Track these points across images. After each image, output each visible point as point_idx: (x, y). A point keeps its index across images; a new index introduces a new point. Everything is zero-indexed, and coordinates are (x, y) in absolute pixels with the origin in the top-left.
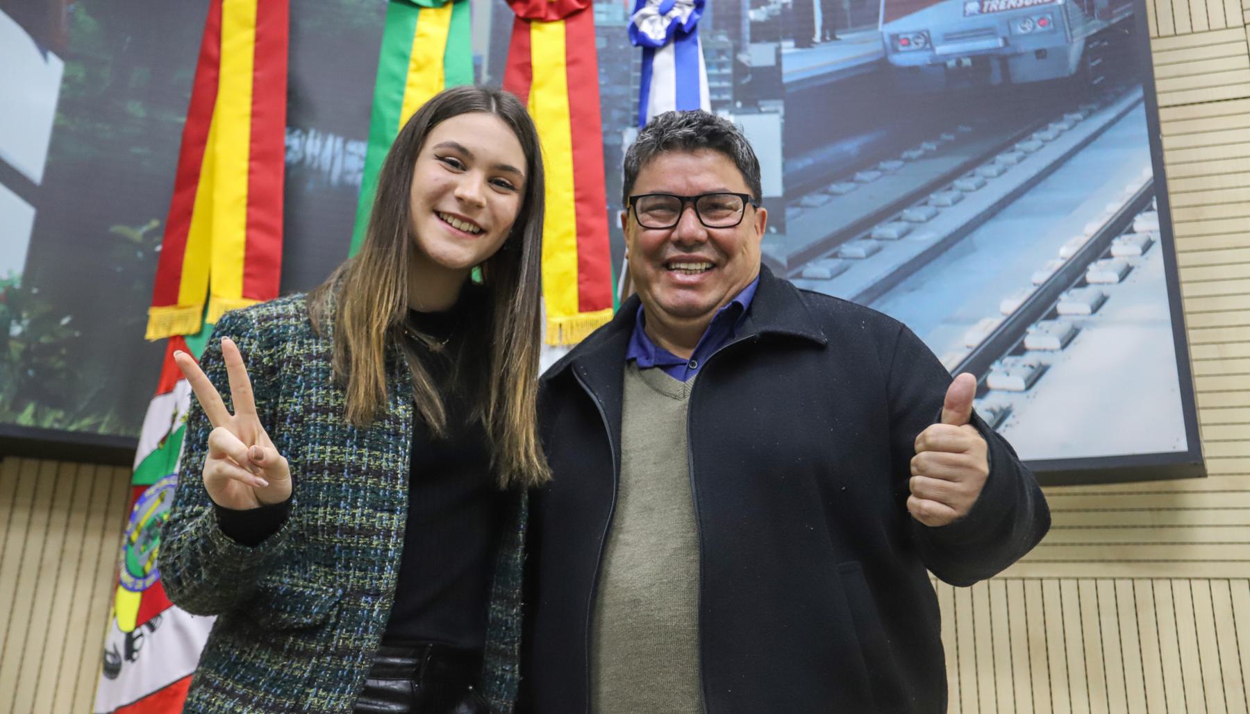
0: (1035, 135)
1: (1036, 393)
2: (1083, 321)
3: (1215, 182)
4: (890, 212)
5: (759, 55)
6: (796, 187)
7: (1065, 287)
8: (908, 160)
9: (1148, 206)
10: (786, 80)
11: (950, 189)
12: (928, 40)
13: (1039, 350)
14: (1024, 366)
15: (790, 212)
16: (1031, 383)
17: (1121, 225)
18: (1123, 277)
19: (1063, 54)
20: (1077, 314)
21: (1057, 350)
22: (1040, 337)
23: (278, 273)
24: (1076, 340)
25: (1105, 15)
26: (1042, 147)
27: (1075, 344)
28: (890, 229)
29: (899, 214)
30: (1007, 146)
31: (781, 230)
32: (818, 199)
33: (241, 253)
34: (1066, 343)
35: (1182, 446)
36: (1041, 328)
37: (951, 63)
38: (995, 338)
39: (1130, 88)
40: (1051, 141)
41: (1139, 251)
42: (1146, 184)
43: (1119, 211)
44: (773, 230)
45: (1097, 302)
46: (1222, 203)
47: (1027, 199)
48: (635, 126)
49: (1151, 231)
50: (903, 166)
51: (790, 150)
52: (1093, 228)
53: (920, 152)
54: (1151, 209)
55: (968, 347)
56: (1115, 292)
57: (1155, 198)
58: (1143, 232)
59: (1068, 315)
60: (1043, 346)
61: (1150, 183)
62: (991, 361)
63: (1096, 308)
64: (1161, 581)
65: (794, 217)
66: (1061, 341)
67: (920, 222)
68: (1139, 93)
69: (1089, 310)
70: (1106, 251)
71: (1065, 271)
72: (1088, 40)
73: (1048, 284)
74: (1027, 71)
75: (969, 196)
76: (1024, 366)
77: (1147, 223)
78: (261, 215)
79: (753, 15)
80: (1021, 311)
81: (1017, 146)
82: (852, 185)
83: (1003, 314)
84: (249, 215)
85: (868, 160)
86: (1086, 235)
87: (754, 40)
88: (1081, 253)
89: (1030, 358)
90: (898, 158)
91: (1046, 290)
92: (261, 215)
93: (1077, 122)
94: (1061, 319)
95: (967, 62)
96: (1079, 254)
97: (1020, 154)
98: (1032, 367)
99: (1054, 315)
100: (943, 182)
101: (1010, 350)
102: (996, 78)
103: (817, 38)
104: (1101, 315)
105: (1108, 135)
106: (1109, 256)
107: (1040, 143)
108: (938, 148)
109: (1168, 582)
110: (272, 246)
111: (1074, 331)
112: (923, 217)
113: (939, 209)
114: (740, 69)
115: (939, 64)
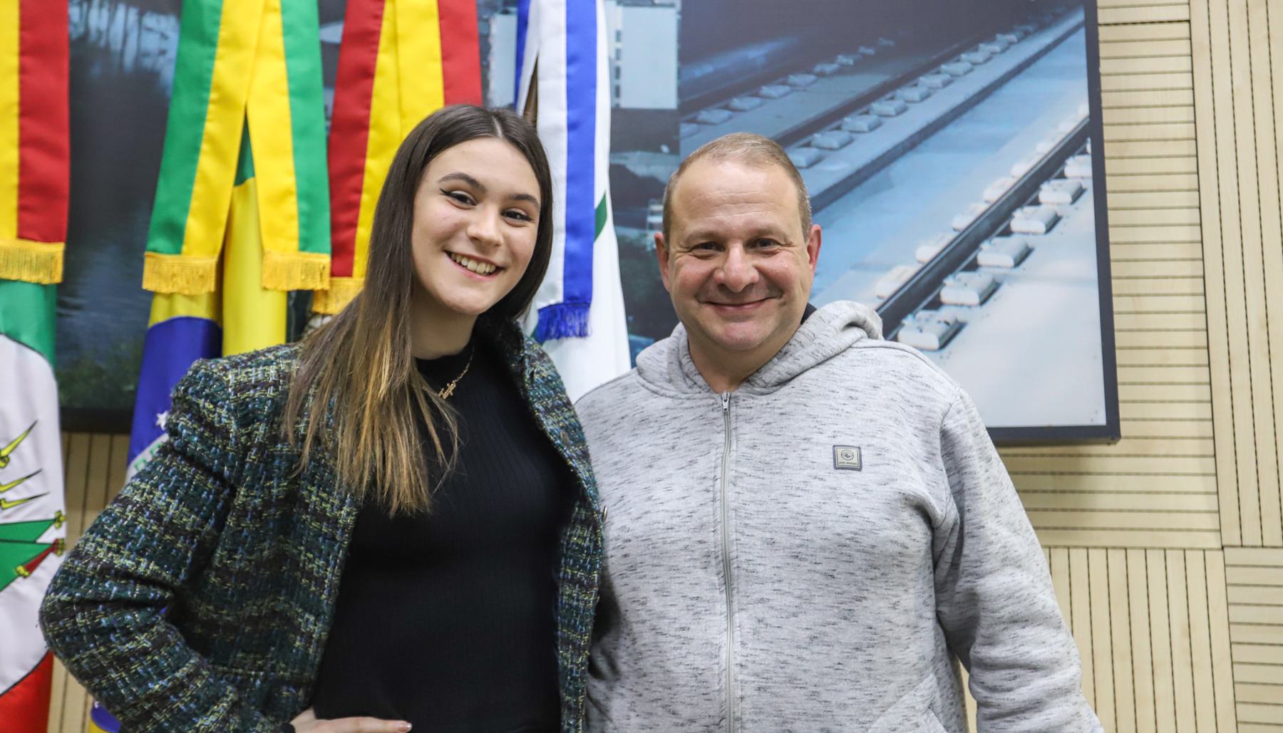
0: (963, 56)
1: (950, 353)
2: (1005, 275)
3: (1143, 115)
7: (987, 235)
8: (821, 75)
9: (1081, 149)
11: (867, 113)
13: (956, 305)
14: (939, 322)
15: (685, 129)
16: (945, 342)
18: (1050, 228)
20: (998, 267)
21: (976, 306)
22: (960, 290)
23: (65, 207)
24: (995, 296)
26: (971, 70)
27: (995, 300)
29: (809, 138)
30: (932, 67)
33: (14, 179)
34: (986, 298)
35: (1101, 420)
36: (959, 280)
38: (909, 289)
39: (1070, 10)
40: (980, 64)
41: (1069, 199)
42: (1081, 123)
43: (1052, 151)
44: (665, 149)
45: (1021, 254)
46: (1148, 140)
47: (951, 131)
48: (506, 12)
49: (1082, 178)
50: (815, 82)
52: (1021, 169)
53: (835, 66)
54: (1084, 152)
55: (879, 297)
56: (1040, 242)
57: (1089, 140)
58: (1074, 178)
59: (989, 266)
60: (960, 301)
61: (1086, 122)
62: (904, 315)
63: (1019, 261)
64: (1058, 550)
65: (691, 135)
66: (980, 296)
67: (831, 149)
68: (1079, 17)
69: (1012, 263)
70: (1033, 197)
71: (991, 214)
73: (970, 230)
75: (888, 121)
76: (939, 322)
77: (1079, 168)
78: (37, 129)
80: (939, 259)
81: (944, 67)
82: (757, 101)
83: (919, 262)
84: (22, 129)
85: (776, 72)
86: (1013, 177)
88: (1007, 196)
89: (945, 314)
90: (809, 72)
91: (967, 236)
92: (37, 129)
93: (1011, 43)
94: (981, 270)
96: (1004, 199)
97: (947, 77)
98: (947, 323)
99: (974, 266)
100: (860, 104)
101: (925, 303)
104: (1024, 269)
105: (1042, 62)
106: (1036, 203)
107: (968, 65)
108: (856, 63)
109: (1066, 550)
110: (57, 170)
111: (994, 286)
112: (835, 144)
113: (854, 135)
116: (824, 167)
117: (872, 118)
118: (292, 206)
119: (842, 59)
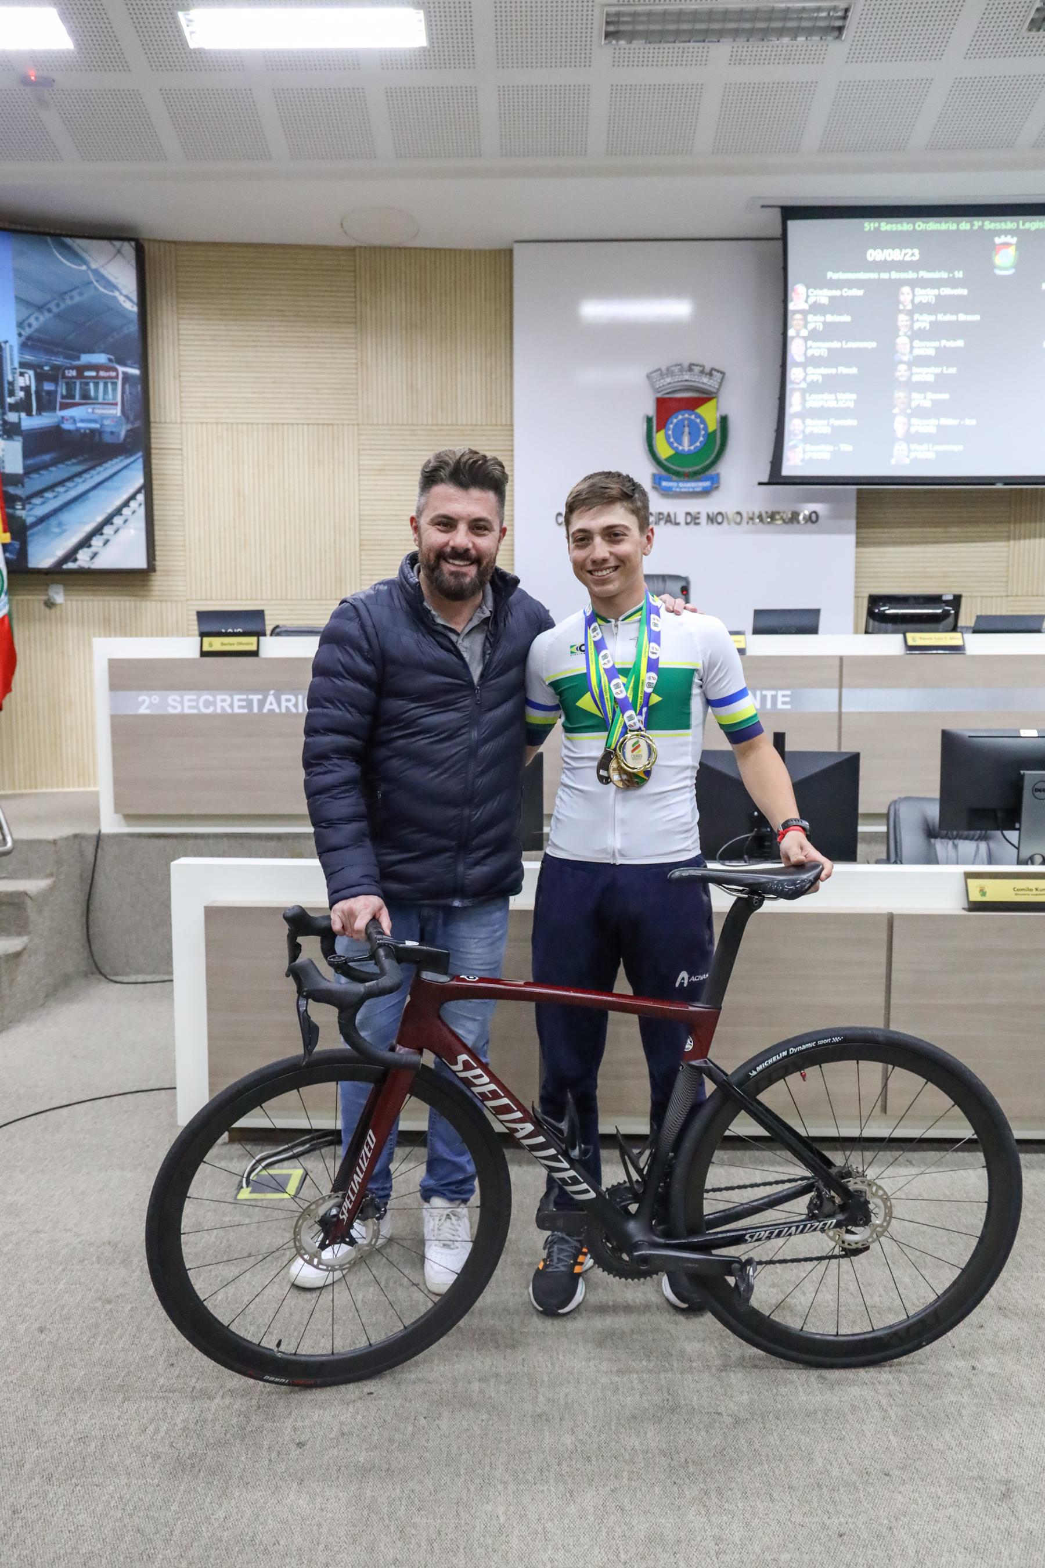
4: (61, 483)
5: (12, 417)
6: (29, 471)
10: (23, 428)
12: (75, 420)
15: (26, 480)
17: (133, 497)
19: (119, 434)
22: (108, 530)
25: (133, 423)
28: (61, 489)
30: (100, 465)
31: (23, 486)
32: (35, 476)
34: (116, 532)
37: (82, 431)
44: (20, 485)
47: (106, 484)
51: (26, 455)
52: (125, 497)
56: (132, 519)
68: (140, 454)
72: (128, 431)
74: (107, 439)
79: (10, 400)
85: (54, 463)
87: (10, 410)
89: (105, 537)
95: (88, 431)
99: (112, 524)
100: (79, 474)
102: (97, 438)
103: (34, 412)
114: (5, 422)
115: (78, 430)
116: (69, 493)
117: (83, 479)
119: (74, 461)
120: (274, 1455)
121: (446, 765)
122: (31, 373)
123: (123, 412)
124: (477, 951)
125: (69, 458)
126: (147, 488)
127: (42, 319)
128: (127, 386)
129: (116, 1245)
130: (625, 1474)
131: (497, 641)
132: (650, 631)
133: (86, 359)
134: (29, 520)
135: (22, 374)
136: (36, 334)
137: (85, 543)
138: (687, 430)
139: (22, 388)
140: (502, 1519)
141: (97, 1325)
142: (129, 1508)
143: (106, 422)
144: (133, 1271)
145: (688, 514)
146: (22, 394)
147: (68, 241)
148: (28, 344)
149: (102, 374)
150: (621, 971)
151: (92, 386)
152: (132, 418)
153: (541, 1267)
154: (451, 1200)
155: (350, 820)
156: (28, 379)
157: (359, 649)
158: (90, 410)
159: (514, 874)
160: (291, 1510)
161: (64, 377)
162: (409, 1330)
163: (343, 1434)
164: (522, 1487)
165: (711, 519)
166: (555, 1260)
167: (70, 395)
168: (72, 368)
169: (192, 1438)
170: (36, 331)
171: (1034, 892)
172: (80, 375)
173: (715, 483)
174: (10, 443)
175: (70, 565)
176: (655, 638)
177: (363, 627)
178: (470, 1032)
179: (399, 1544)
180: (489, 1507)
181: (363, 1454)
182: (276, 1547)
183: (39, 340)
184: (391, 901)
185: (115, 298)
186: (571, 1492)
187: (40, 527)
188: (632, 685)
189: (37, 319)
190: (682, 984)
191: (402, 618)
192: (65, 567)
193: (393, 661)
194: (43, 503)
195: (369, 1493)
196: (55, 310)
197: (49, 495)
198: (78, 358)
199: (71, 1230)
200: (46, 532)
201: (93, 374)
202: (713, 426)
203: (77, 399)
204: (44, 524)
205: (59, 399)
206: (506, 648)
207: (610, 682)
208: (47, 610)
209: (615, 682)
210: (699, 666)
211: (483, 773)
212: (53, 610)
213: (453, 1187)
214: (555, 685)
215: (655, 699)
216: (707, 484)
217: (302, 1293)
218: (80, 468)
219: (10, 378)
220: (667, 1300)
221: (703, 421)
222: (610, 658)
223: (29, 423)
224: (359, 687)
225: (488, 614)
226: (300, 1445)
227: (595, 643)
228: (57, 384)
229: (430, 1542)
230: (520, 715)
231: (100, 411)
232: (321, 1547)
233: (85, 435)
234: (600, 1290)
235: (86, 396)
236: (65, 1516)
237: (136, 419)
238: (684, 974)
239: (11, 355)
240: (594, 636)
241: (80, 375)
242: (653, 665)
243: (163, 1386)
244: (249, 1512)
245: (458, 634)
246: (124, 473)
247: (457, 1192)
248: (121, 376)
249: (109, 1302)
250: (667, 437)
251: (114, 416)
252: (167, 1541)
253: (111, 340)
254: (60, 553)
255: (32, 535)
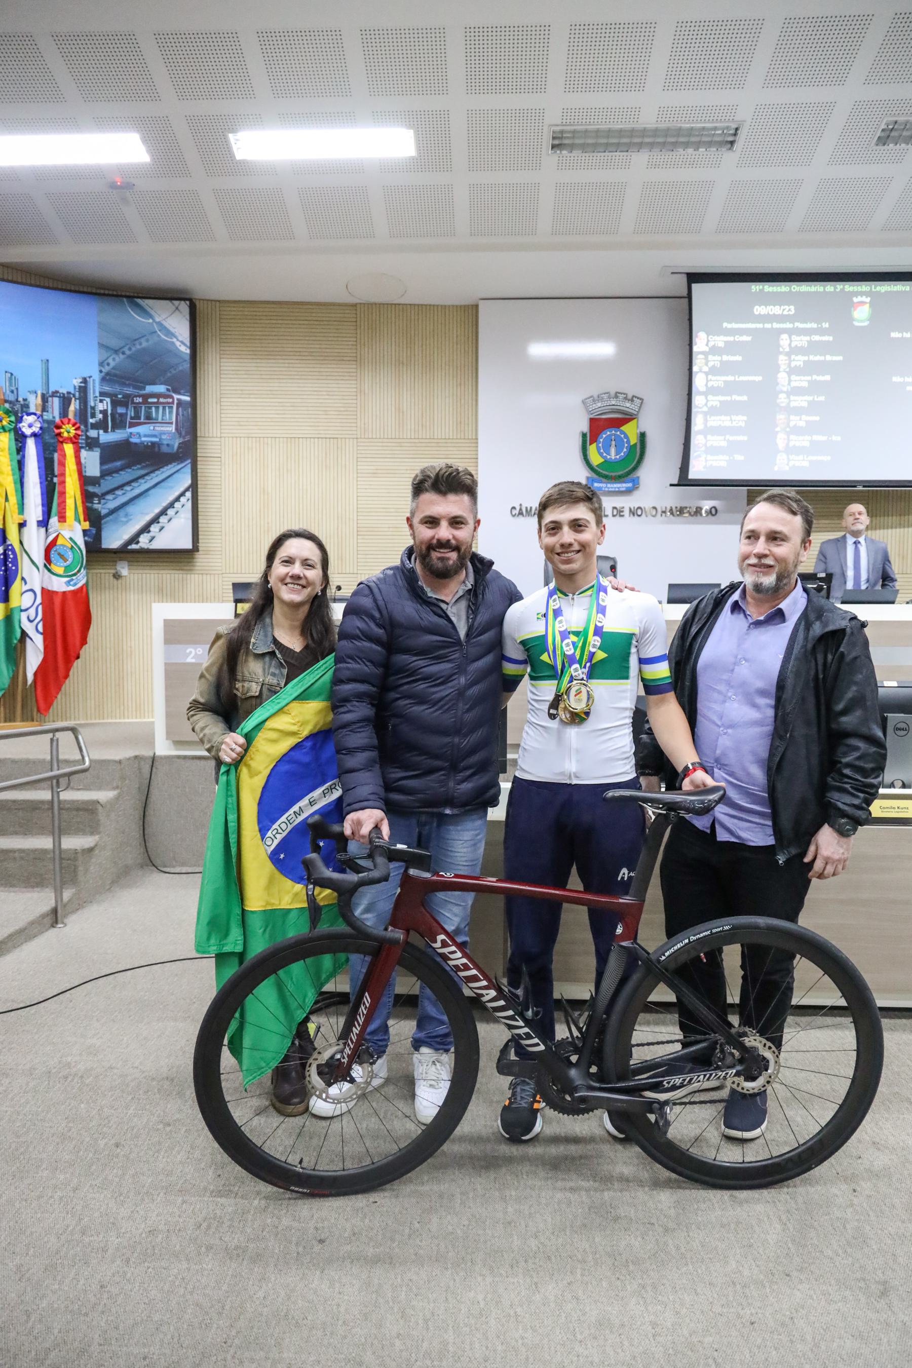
4: (128, 483)
5: (93, 433)
6: (104, 474)
15: (102, 481)
16: (160, 530)
17: (183, 494)
19: (173, 447)
22: (163, 519)
25: (184, 438)
28: (128, 488)
31: (100, 485)
34: (170, 520)
47: (162, 484)
51: (102, 463)
52: (177, 494)
56: (181, 511)
68: (189, 461)
74: (165, 449)
79: (91, 421)
85: (123, 468)
87: (92, 428)
89: (160, 525)
100: (142, 477)
102: (156, 449)
114: (87, 437)
115: (142, 443)
118: (16, 506)
119: (139, 466)
120: (301, 1249)
121: (440, 704)
122: (108, 400)
123: (177, 429)
124: (462, 850)
125: (134, 465)
126: (194, 487)
127: (117, 359)
128: (180, 409)
129: (172, 1080)
130: (579, 1271)
131: (477, 609)
132: (598, 604)
133: (150, 389)
134: (104, 512)
135: (101, 401)
136: (114, 371)
137: (146, 529)
138: (613, 443)
139: (101, 412)
140: (482, 1304)
141: (160, 1143)
142: (190, 1287)
143: (164, 437)
144: (186, 1101)
145: (614, 508)
146: (101, 416)
147: (139, 301)
148: (107, 378)
149: (162, 400)
150: (574, 869)
151: (153, 409)
152: (183, 433)
153: (507, 1103)
154: (437, 1049)
155: (363, 749)
156: (105, 405)
157: (372, 618)
158: (152, 428)
159: (492, 792)
160: (315, 1292)
161: (133, 402)
162: (403, 1152)
163: (354, 1234)
164: (497, 1279)
165: (633, 512)
166: (519, 1098)
167: (137, 416)
168: (139, 396)
169: (236, 1233)
170: (113, 368)
171: (897, 810)
172: (145, 401)
173: (636, 485)
174: (90, 453)
175: (134, 546)
176: (602, 610)
177: (375, 601)
178: (456, 915)
179: (402, 1322)
180: (472, 1294)
181: (371, 1250)
182: (305, 1322)
183: (115, 375)
184: (391, 809)
185: (173, 343)
186: (536, 1284)
187: (111, 517)
188: (580, 645)
189: (114, 359)
190: (623, 878)
191: (405, 593)
192: (129, 547)
193: (400, 625)
194: (114, 499)
195: (376, 1281)
196: (128, 352)
197: (119, 492)
198: (144, 389)
199: (137, 1068)
200: (116, 521)
201: (155, 400)
202: (634, 440)
203: (142, 420)
204: (114, 515)
205: (128, 419)
206: (483, 617)
207: (562, 641)
208: (115, 581)
209: (566, 641)
210: (637, 631)
211: (468, 711)
212: (120, 581)
213: (438, 1040)
214: (523, 643)
215: (601, 655)
216: (630, 485)
217: (319, 1122)
218: (143, 472)
219: (92, 404)
220: (608, 1132)
221: (626, 436)
222: (564, 623)
223: (106, 437)
224: (374, 646)
225: (470, 587)
226: (321, 1241)
227: (554, 610)
228: (127, 408)
229: (426, 1321)
230: (496, 667)
231: (159, 428)
232: (340, 1322)
233: (147, 447)
234: (554, 1124)
235: (149, 417)
236: (141, 1292)
237: (187, 434)
238: (625, 871)
239: (94, 386)
240: (553, 605)
241: (145, 401)
242: (598, 631)
243: (213, 1192)
244: (283, 1293)
245: (447, 604)
246: (174, 476)
247: (438, 1043)
248: (176, 402)
249: (169, 1125)
250: (598, 448)
251: (169, 433)
252: (220, 1314)
253: (169, 374)
254: (126, 537)
255: (105, 523)
